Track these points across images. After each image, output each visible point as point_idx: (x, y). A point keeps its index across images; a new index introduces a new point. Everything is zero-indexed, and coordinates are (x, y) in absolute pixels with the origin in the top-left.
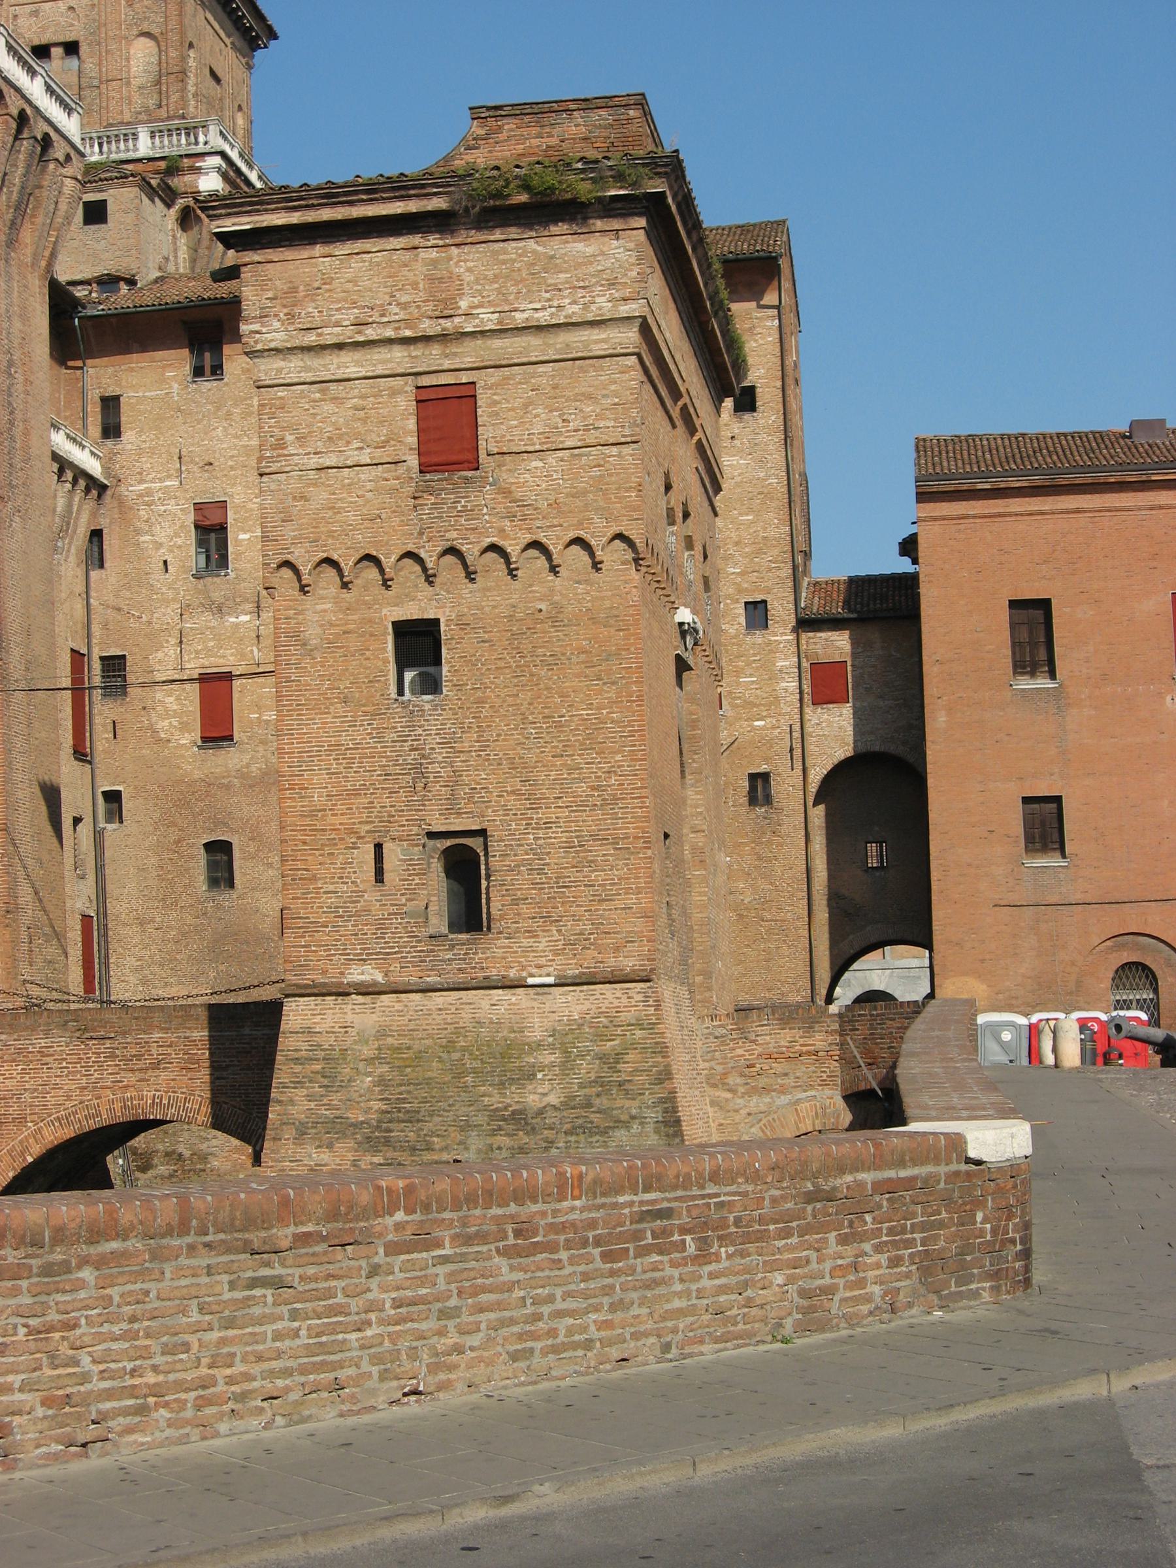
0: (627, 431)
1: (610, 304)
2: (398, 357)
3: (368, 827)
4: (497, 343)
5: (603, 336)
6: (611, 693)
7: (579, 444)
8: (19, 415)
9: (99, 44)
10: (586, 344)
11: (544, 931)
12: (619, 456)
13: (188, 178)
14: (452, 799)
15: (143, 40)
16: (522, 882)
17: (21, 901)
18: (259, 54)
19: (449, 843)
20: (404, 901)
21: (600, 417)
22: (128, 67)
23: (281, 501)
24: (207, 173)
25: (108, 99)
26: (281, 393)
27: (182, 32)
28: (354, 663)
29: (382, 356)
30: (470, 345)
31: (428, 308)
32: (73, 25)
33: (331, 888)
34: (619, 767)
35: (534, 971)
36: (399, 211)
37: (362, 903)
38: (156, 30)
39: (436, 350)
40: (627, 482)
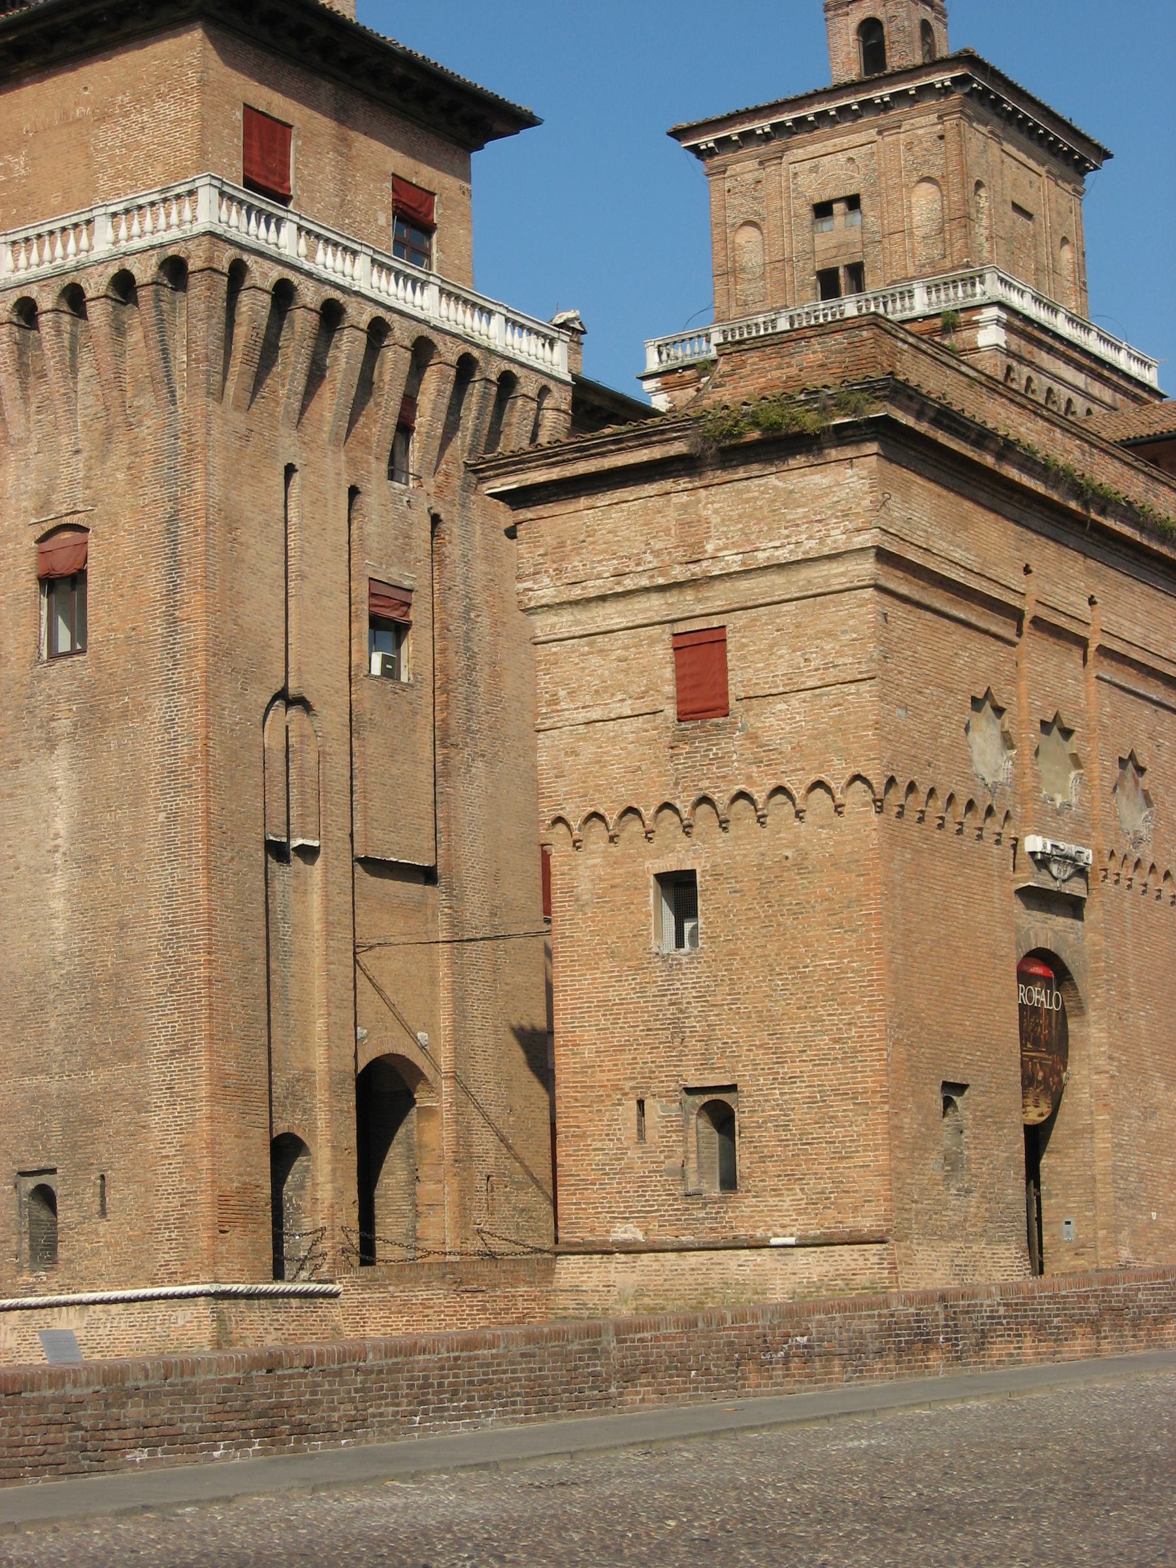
0: (864, 668)
1: (844, 537)
2: (655, 605)
3: (632, 1083)
4: (744, 584)
5: (842, 569)
6: (852, 941)
7: (819, 684)
8: (482, 659)
9: (880, 195)
10: (827, 578)
11: (788, 1190)
12: (858, 693)
13: (966, 334)
14: (706, 1055)
15: (925, 186)
16: (768, 1138)
17: (477, 1149)
18: (1089, 176)
19: (707, 1098)
20: (663, 1158)
21: (840, 653)
22: (911, 217)
23: (555, 758)
24: (985, 327)
25: (891, 255)
26: (555, 648)
27: (964, 173)
28: (620, 918)
29: (642, 606)
30: (720, 587)
31: (678, 554)
32: (852, 177)
33: (599, 1145)
34: (859, 1018)
35: (779, 1230)
36: (645, 459)
37: (626, 1161)
38: (936, 174)
39: (689, 595)
40: (865, 721)
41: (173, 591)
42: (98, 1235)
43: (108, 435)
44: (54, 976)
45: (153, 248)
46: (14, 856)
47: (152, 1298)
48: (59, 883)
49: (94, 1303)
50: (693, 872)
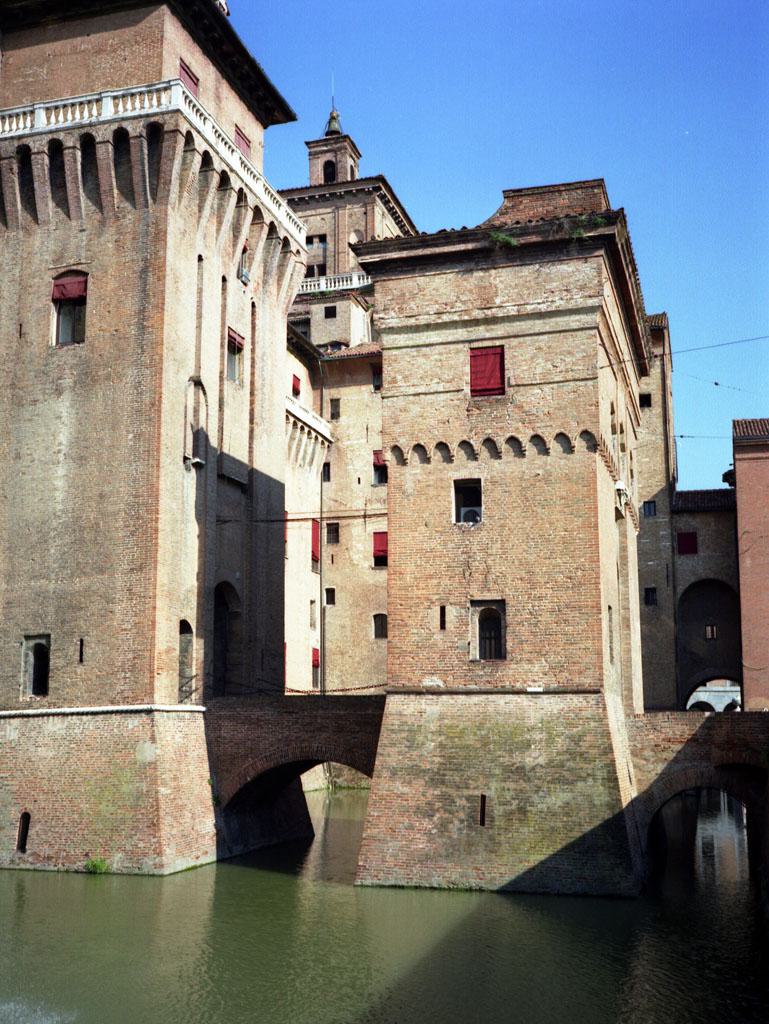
2: (461, 333)
3: (437, 597)
16: (524, 630)
23: (394, 413)
26: (395, 352)
33: (415, 631)
41: (142, 311)
42: (76, 674)
43: (103, 223)
44: (55, 524)
45: (141, 116)
46: (31, 454)
47: (112, 712)
48: (61, 471)
49: (72, 714)
50: (479, 480)
